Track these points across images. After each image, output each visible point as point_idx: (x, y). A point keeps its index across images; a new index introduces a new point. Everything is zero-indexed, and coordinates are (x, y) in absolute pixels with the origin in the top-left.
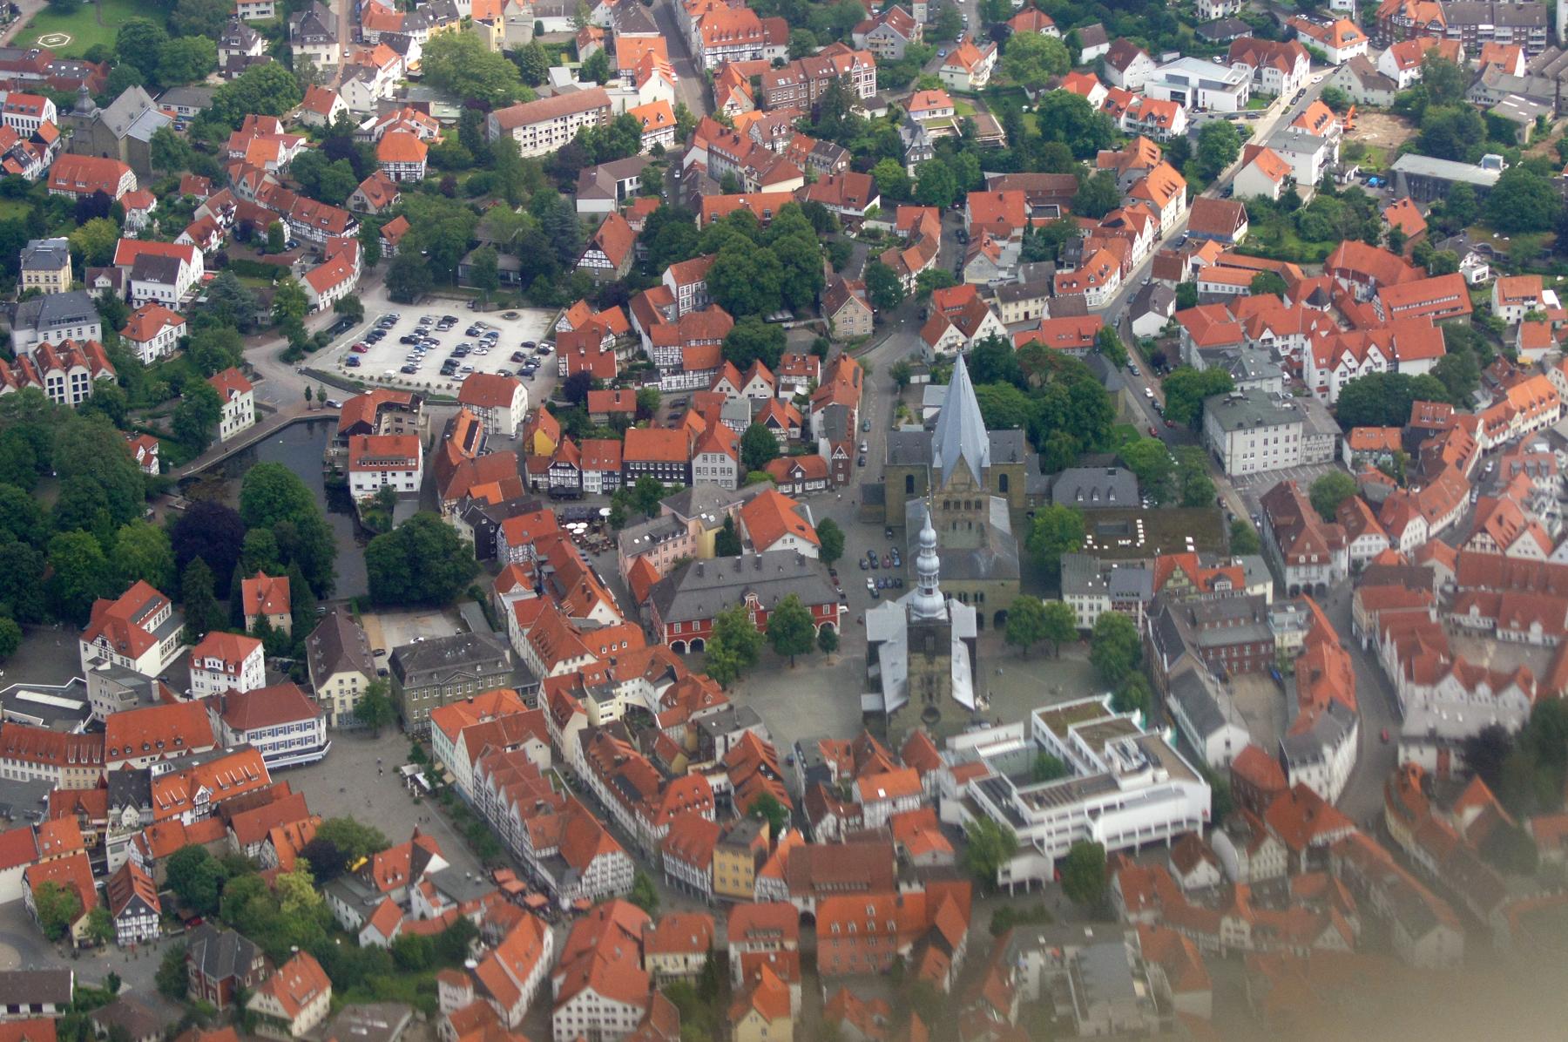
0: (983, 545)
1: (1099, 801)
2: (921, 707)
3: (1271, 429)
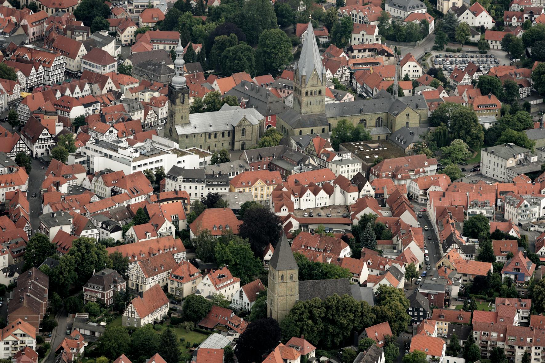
0: (300, 113)
1: (109, 152)
2: (169, 127)
3: (497, 157)
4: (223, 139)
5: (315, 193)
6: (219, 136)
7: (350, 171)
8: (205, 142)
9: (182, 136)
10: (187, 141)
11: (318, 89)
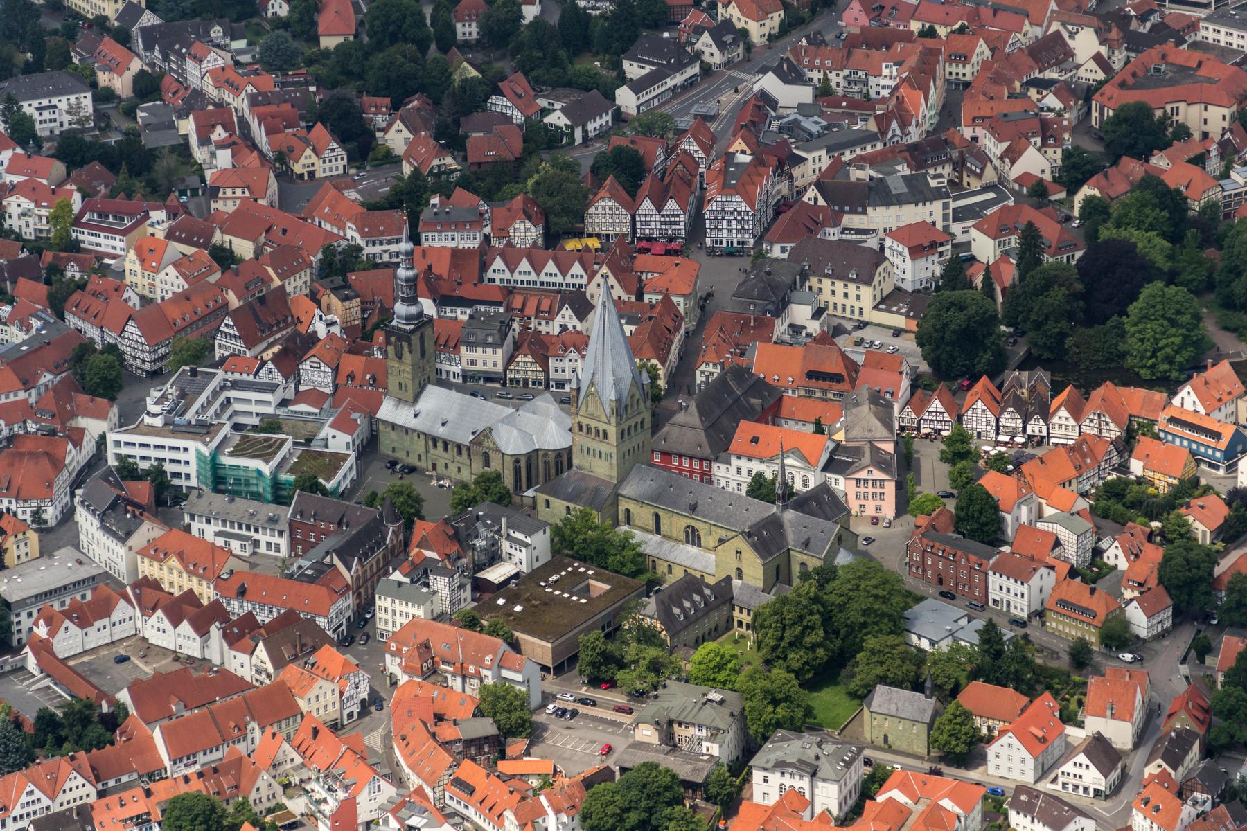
4: (458, 458)
5: (175, 624)
6: (453, 451)
7: (398, 613)
8: (427, 452)
9: (384, 422)
10: (393, 435)
11: (601, 427)
